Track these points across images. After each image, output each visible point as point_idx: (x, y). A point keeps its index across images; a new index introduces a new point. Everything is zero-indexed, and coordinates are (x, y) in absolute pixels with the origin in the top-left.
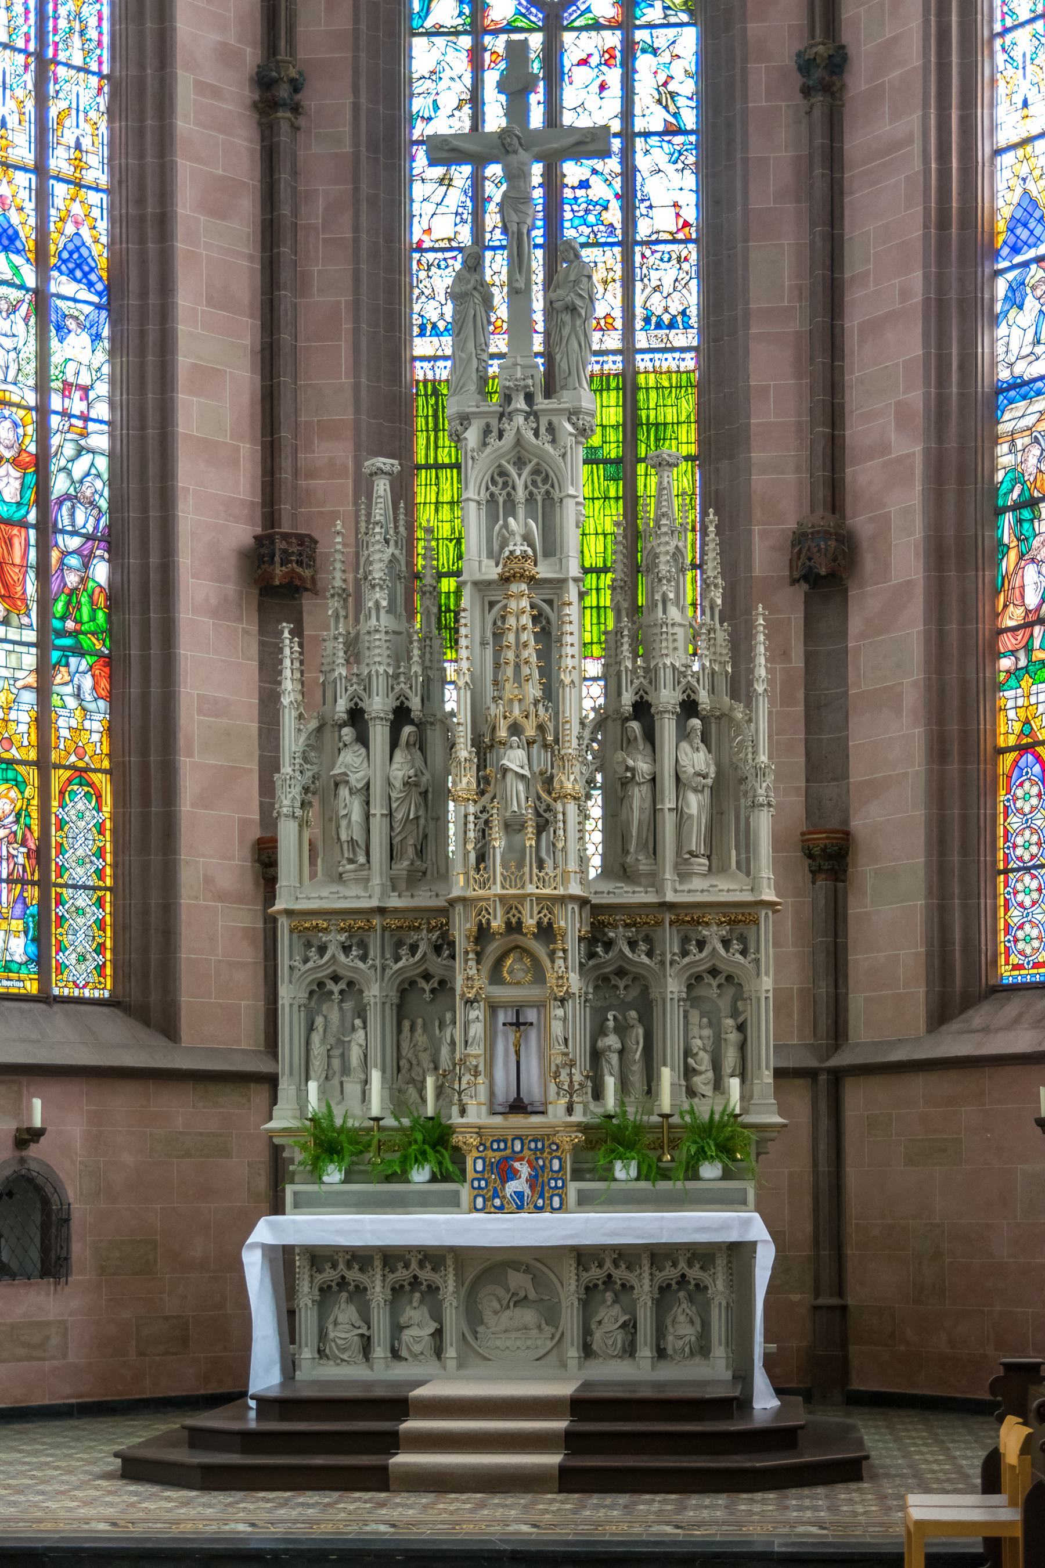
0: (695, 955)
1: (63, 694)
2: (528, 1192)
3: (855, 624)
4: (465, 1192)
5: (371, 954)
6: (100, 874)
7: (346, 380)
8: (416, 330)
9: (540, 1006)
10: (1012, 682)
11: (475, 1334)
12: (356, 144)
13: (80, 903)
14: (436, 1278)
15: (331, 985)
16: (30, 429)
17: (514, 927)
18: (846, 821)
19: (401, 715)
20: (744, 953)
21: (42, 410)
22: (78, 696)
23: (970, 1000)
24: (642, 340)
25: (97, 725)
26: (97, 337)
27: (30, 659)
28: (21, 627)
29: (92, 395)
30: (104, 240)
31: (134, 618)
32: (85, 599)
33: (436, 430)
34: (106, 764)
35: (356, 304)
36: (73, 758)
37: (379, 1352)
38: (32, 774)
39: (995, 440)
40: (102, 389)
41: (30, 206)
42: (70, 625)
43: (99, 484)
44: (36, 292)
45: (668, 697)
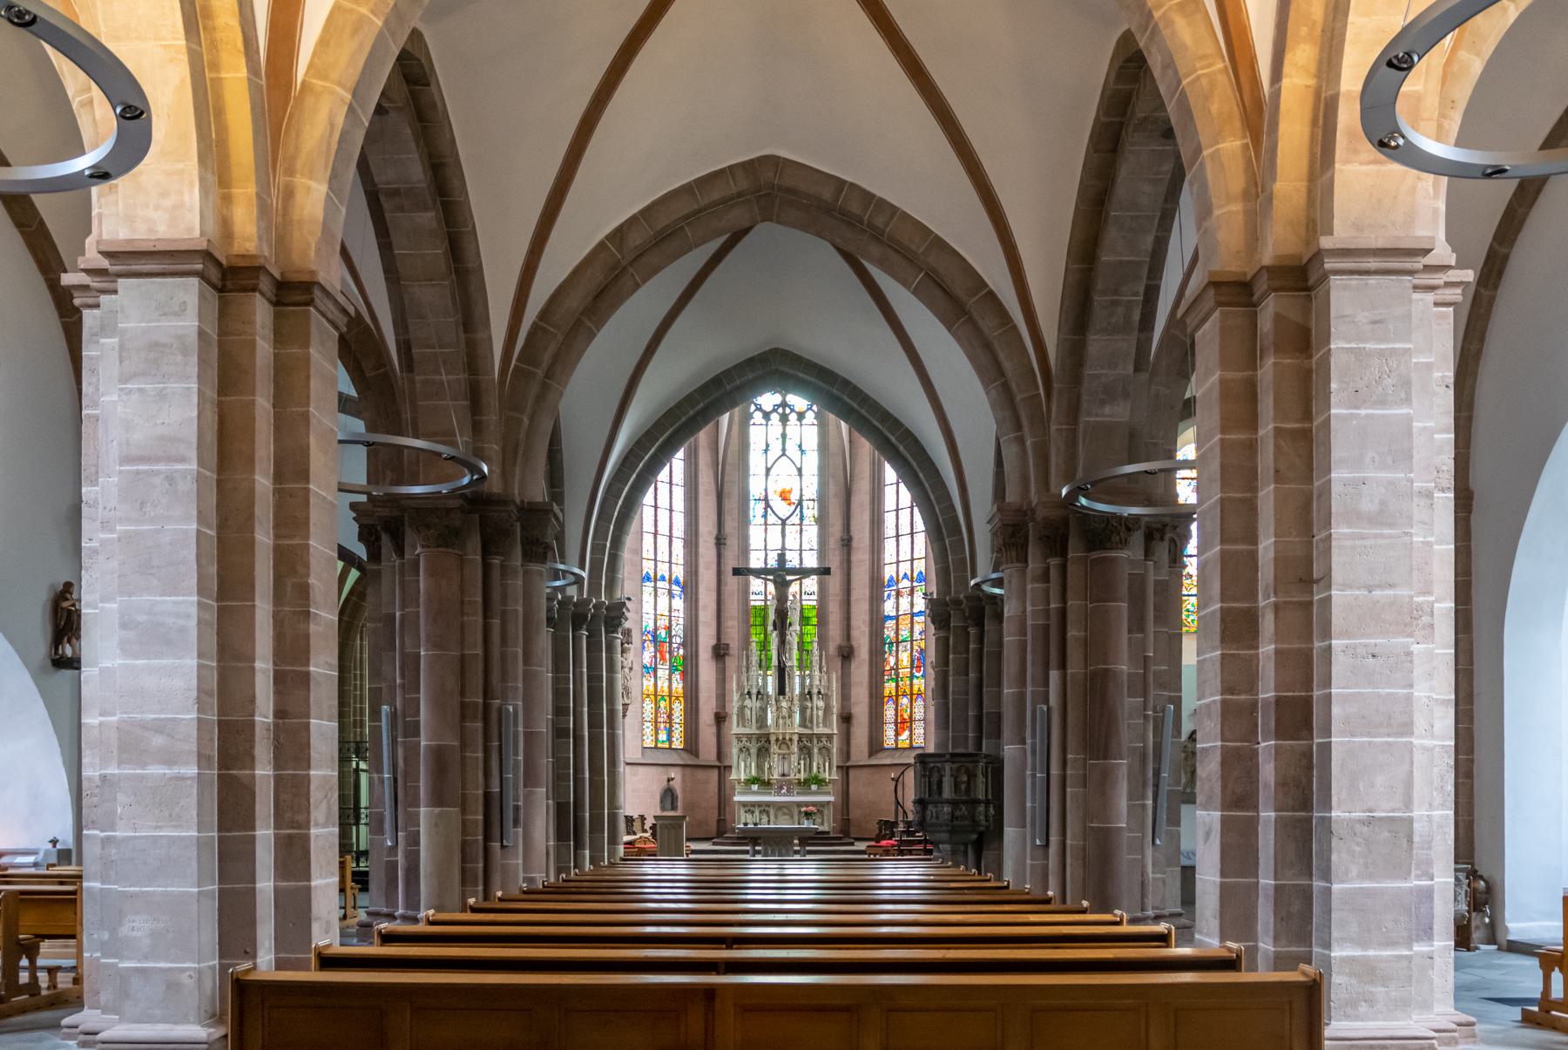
1: (674, 680)
3: (853, 667)
7: (736, 606)
9: (789, 754)
17: (784, 739)
19: (759, 693)
21: (670, 616)
24: (804, 597)
25: (681, 685)
27: (667, 672)
31: (689, 662)
38: (668, 699)
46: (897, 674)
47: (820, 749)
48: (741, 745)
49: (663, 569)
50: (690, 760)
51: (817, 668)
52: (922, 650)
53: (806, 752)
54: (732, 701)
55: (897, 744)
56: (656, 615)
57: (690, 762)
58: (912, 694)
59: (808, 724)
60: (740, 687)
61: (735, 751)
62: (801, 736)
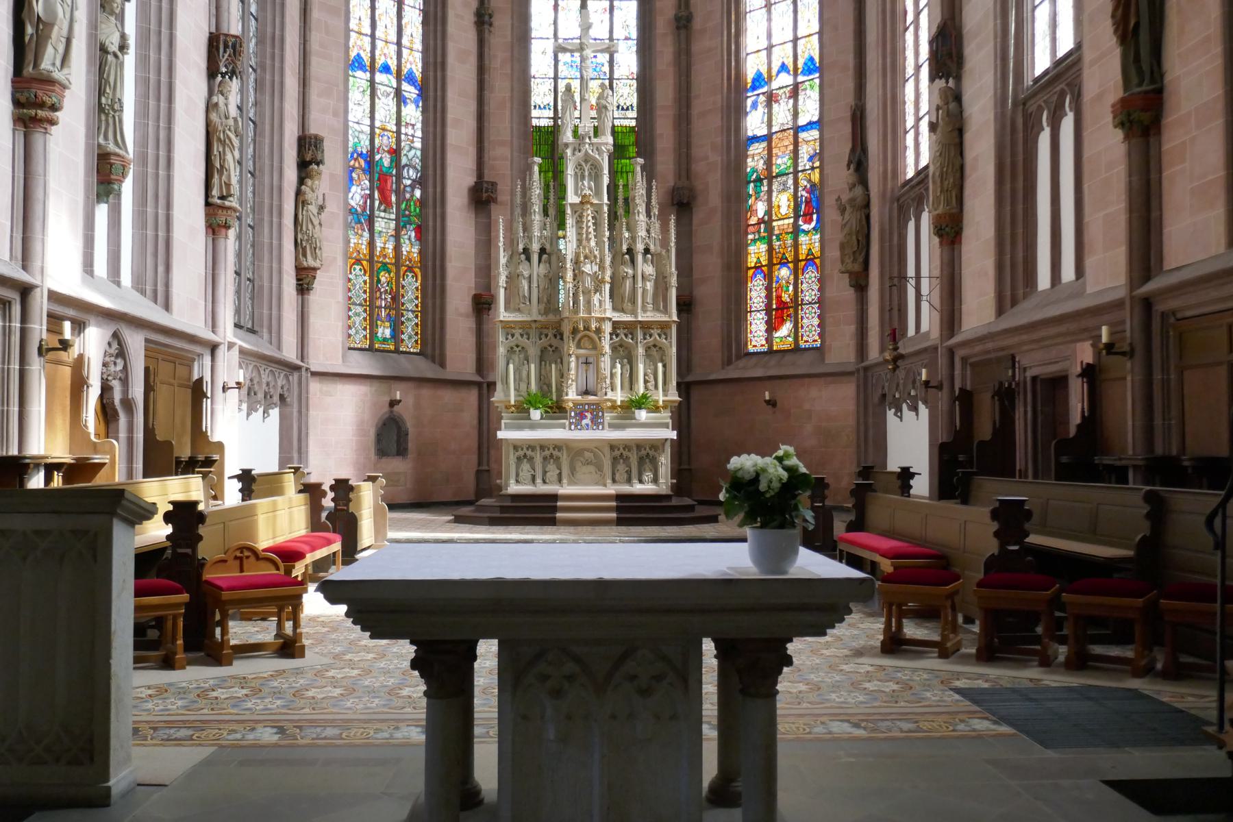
0: (649, 340)
1: (405, 241)
2: (590, 424)
3: (695, 221)
4: (567, 422)
5: (531, 336)
6: (417, 306)
7: (507, 124)
8: (533, 107)
10: (753, 244)
11: (573, 474)
12: (512, 38)
13: (410, 317)
14: (559, 454)
15: (515, 348)
16: (394, 140)
18: (691, 293)
19: (543, 251)
20: (666, 339)
21: (398, 133)
22: (409, 239)
23: (739, 357)
25: (415, 250)
26: (417, 106)
27: (393, 225)
28: (390, 213)
29: (415, 127)
30: (420, 70)
31: (431, 211)
32: (412, 203)
33: (540, 145)
34: (419, 265)
35: (512, 97)
36: (408, 263)
37: (539, 481)
38: (393, 268)
39: (747, 157)
40: (419, 126)
41: (395, 57)
42: (407, 213)
43: (418, 161)
44: (397, 89)
45: (640, 247)
46: (770, 230)
47: (648, 349)
48: (512, 341)
49: (386, 54)
50: (425, 368)
51: (642, 208)
52: (813, 185)
53: (624, 353)
54: (498, 268)
55: (771, 346)
56: (372, 127)
57: (430, 375)
58: (796, 260)
59: (628, 306)
60: (511, 242)
61: (502, 350)
62: (616, 325)
